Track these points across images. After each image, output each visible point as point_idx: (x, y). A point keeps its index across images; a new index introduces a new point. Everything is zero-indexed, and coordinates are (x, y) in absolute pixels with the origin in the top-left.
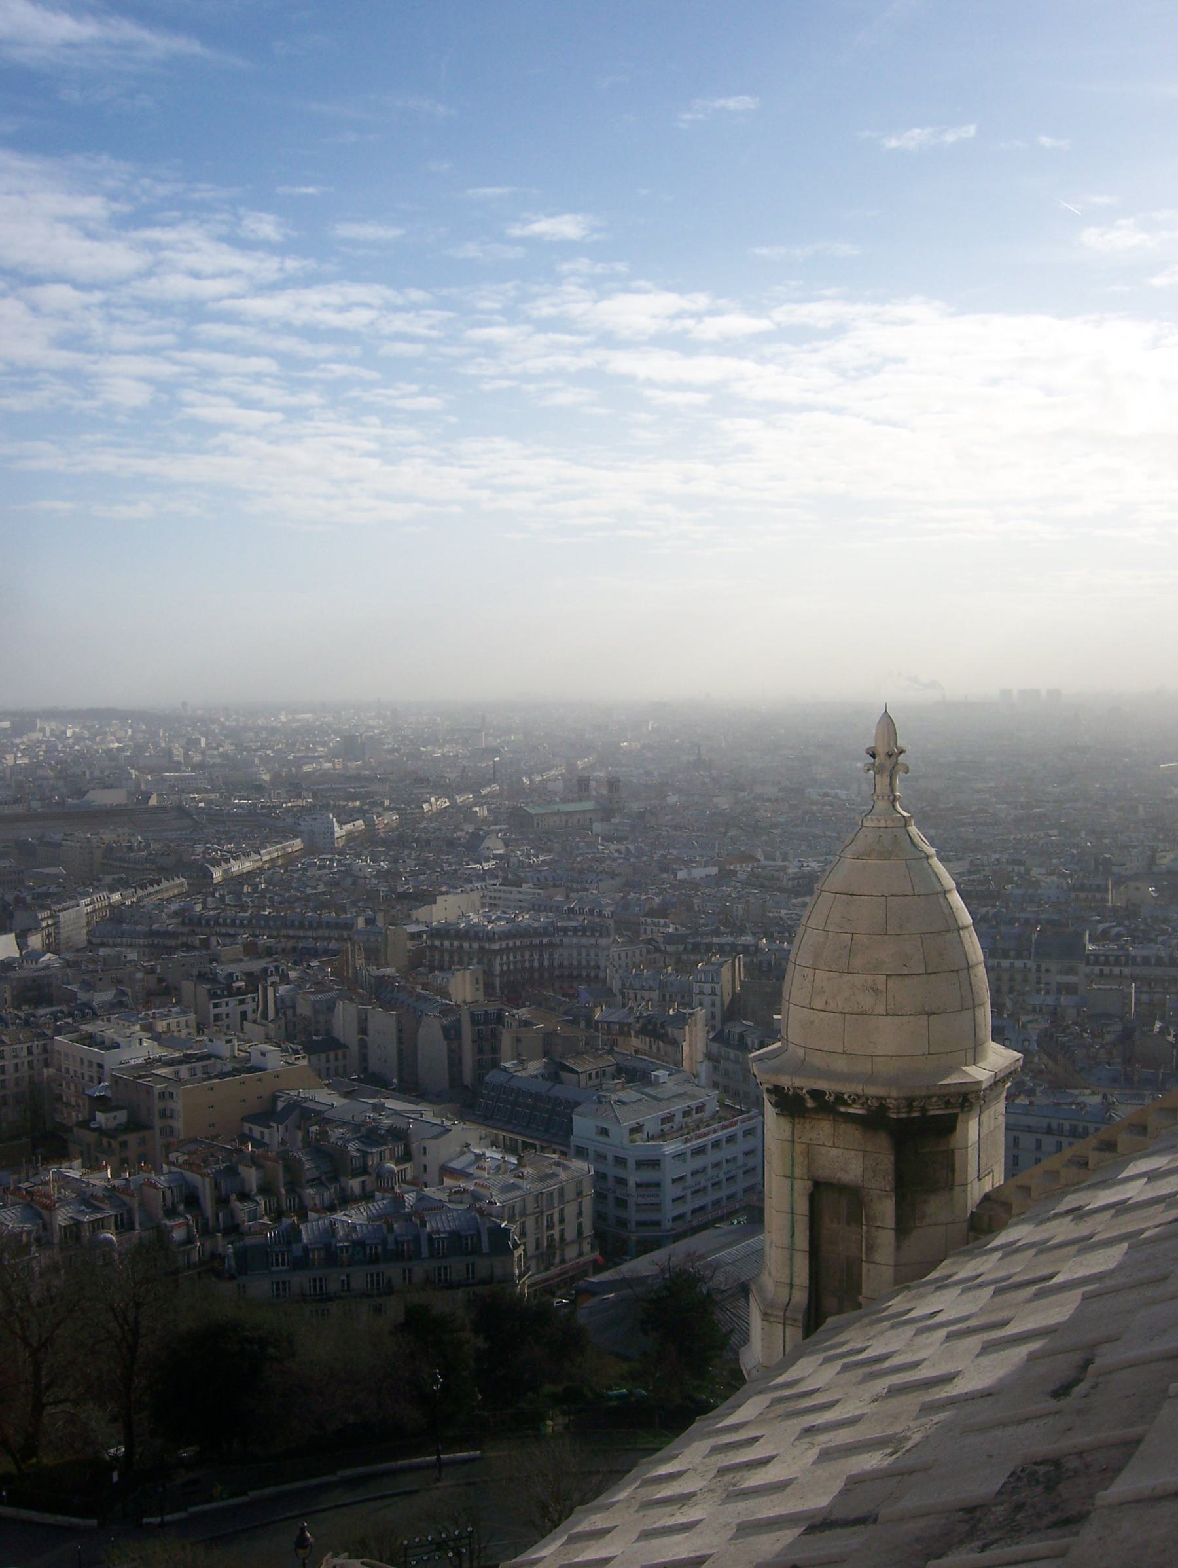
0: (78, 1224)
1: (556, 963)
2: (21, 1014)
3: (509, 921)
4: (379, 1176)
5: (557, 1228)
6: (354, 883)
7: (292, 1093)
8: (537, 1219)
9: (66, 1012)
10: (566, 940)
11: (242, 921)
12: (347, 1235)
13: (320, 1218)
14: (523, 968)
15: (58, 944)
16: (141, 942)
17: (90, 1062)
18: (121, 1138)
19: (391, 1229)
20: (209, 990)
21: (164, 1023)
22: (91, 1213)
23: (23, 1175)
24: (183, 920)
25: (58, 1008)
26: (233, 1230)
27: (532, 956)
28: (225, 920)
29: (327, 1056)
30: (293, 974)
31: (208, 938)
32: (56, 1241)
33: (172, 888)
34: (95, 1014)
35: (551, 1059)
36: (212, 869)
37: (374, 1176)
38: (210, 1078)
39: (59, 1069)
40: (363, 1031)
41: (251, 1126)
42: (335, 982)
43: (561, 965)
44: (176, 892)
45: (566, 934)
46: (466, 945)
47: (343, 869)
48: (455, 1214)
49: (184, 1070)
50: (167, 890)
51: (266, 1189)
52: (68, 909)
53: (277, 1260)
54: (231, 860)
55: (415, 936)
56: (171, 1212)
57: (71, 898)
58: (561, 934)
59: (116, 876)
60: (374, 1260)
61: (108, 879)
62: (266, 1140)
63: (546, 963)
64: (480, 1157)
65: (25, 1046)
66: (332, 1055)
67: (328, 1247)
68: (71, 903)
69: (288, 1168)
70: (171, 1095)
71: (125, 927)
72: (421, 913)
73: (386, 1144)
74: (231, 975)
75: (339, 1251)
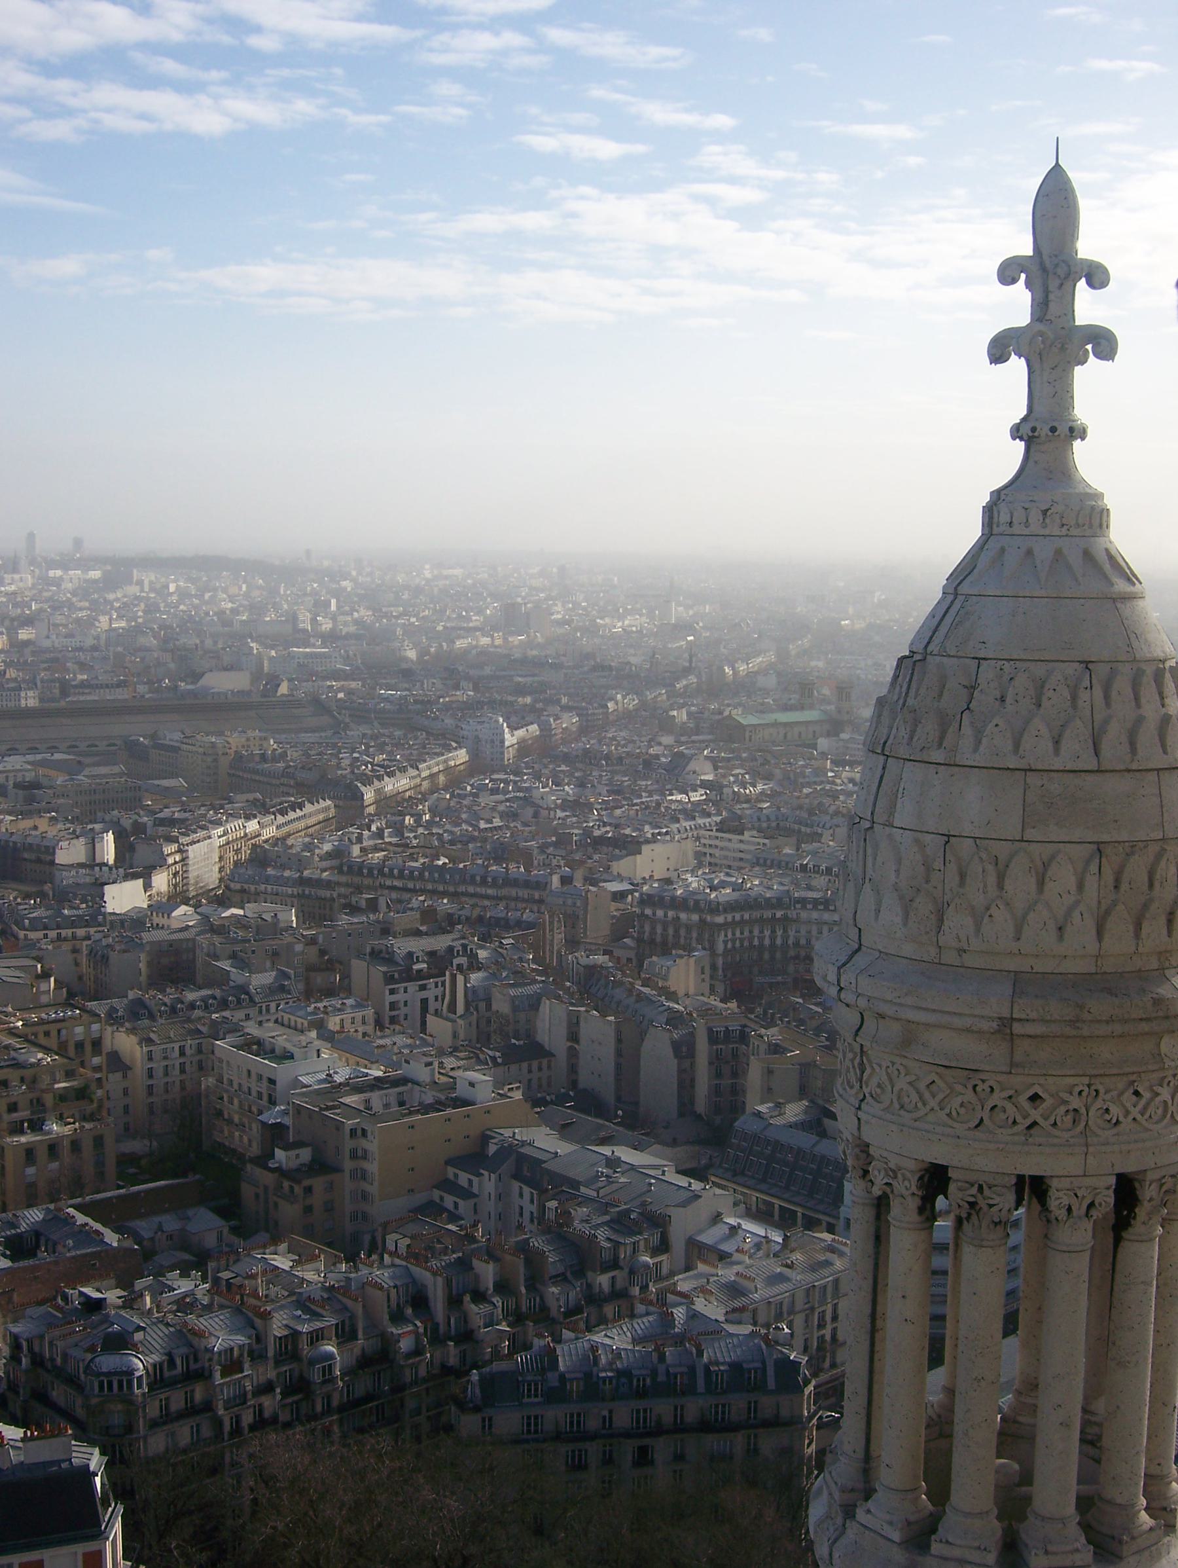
0: (295, 1335)
1: (790, 942)
2: (166, 1000)
3: (736, 888)
4: (632, 1272)
5: (829, 1327)
6: (536, 815)
7: (507, 1133)
8: (807, 1316)
9: (218, 996)
10: (804, 915)
11: (412, 872)
12: (611, 1363)
13: (577, 1339)
14: (752, 946)
15: (187, 884)
16: (290, 891)
17: (260, 1077)
18: (306, 1183)
19: (662, 1358)
20: (385, 973)
21: (337, 1019)
22: (309, 1320)
23: (223, 1262)
24: (341, 865)
25: (209, 992)
26: (466, 1336)
27: (761, 932)
28: (391, 870)
29: (530, 1066)
30: (482, 954)
31: (376, 899)
32: (271, 1353)
33: (319, 812)
34: (251, 1000)
35: (811, 1101)
36: (363, 789)
37: (627, 1270)
38: (411, 1113)
39: (220, 1080)
40: (574, 1037)
41: (457, 1171)
42: (539, 973)
43: (797, 944)
44: (321, 817)
45: (804, 907)
46: (683, 916)
47: (521, 795)
48: (735, 1340)
49: (377, 1099)
50: (310, 815)
51: (503, 1287)
52: (198, 841)
53: (529, 1390)
54: (386, 778)
55: (619, 896)
56: (397, 1317)
57: (203, 828)
58: (798, 906)
59: (251, 796)
60: (641, 1394)
61: (240, 800)
62: (475, 1190)
63: (779, 942)
64: (734, 1229)
65: (177, 1046)
66: (535, 1064)
67: (588, 1376)
68: (201, 834)
69: (528, 1262)
70: (364, 1132)
71: (270, 871)
72: (621, 866)
73: (640, 1233)
74: (410, 955)
75: (601, 1382)
